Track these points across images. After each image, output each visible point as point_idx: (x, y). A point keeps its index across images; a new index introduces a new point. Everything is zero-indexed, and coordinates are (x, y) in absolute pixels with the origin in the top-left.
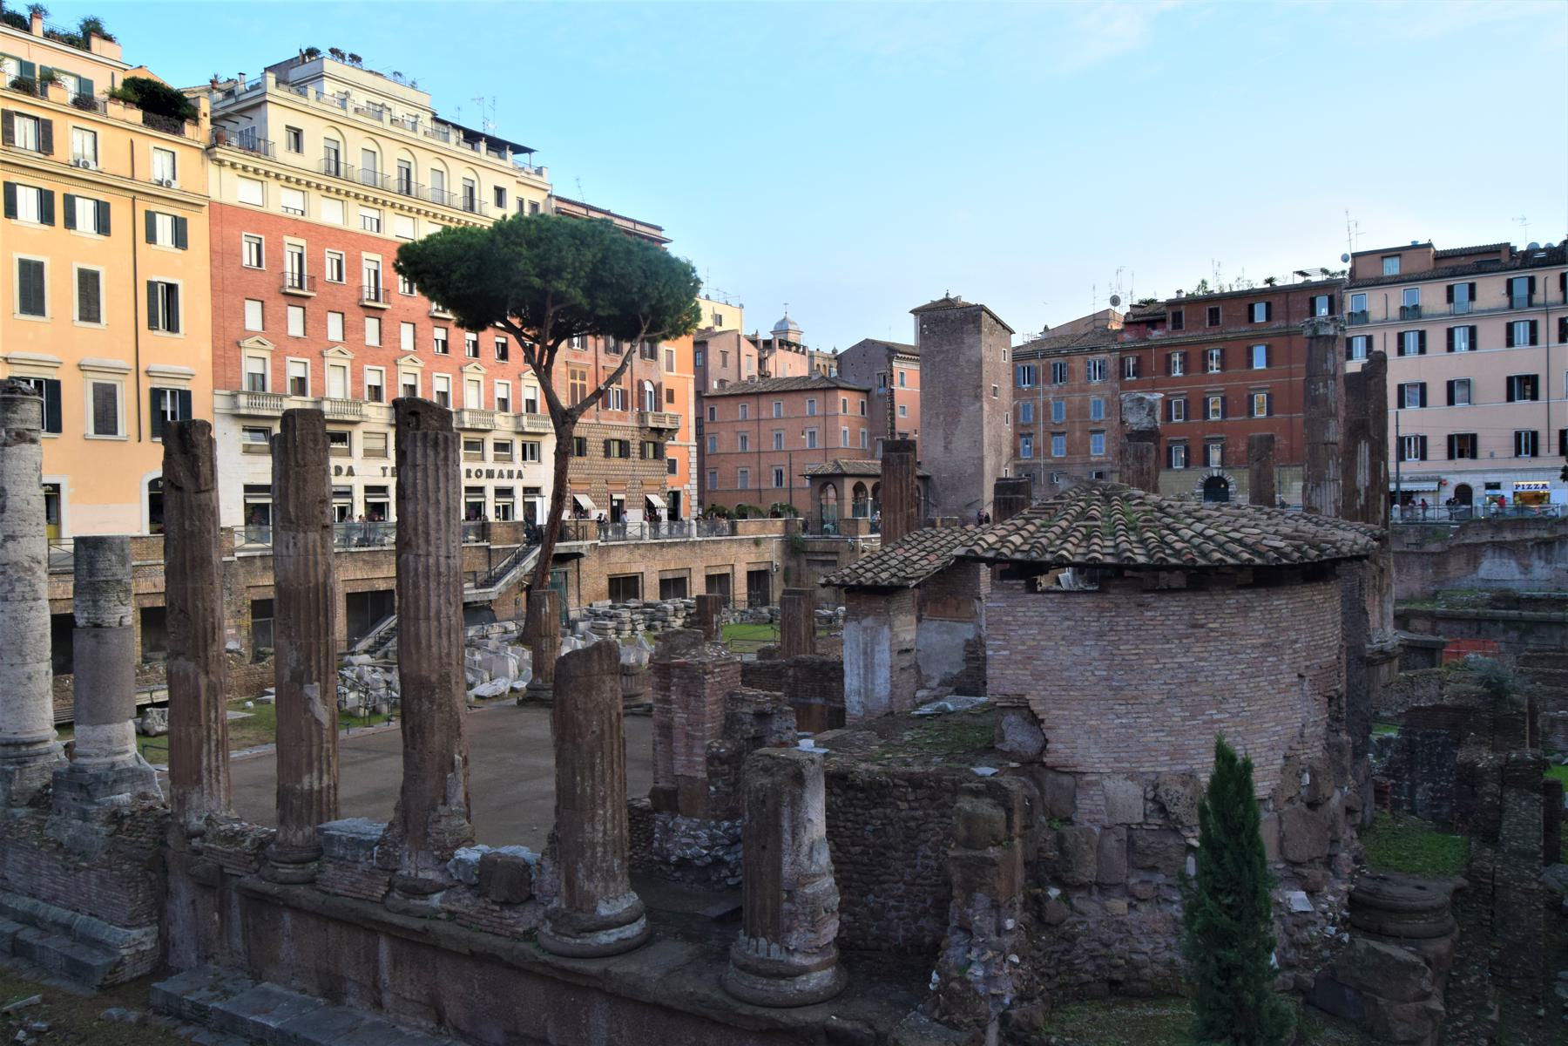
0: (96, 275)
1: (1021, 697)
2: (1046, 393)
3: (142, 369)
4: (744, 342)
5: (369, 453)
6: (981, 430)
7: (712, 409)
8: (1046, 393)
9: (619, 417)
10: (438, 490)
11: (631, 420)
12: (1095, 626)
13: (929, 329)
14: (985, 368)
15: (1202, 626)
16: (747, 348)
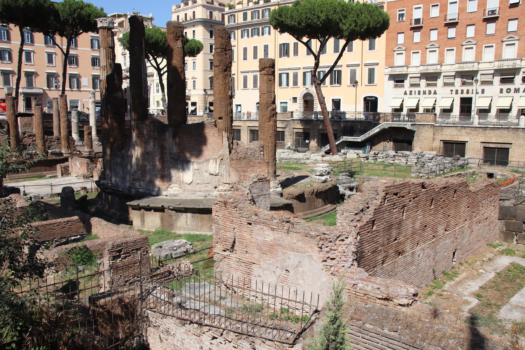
3: (363, 65)
5: (445, 84)
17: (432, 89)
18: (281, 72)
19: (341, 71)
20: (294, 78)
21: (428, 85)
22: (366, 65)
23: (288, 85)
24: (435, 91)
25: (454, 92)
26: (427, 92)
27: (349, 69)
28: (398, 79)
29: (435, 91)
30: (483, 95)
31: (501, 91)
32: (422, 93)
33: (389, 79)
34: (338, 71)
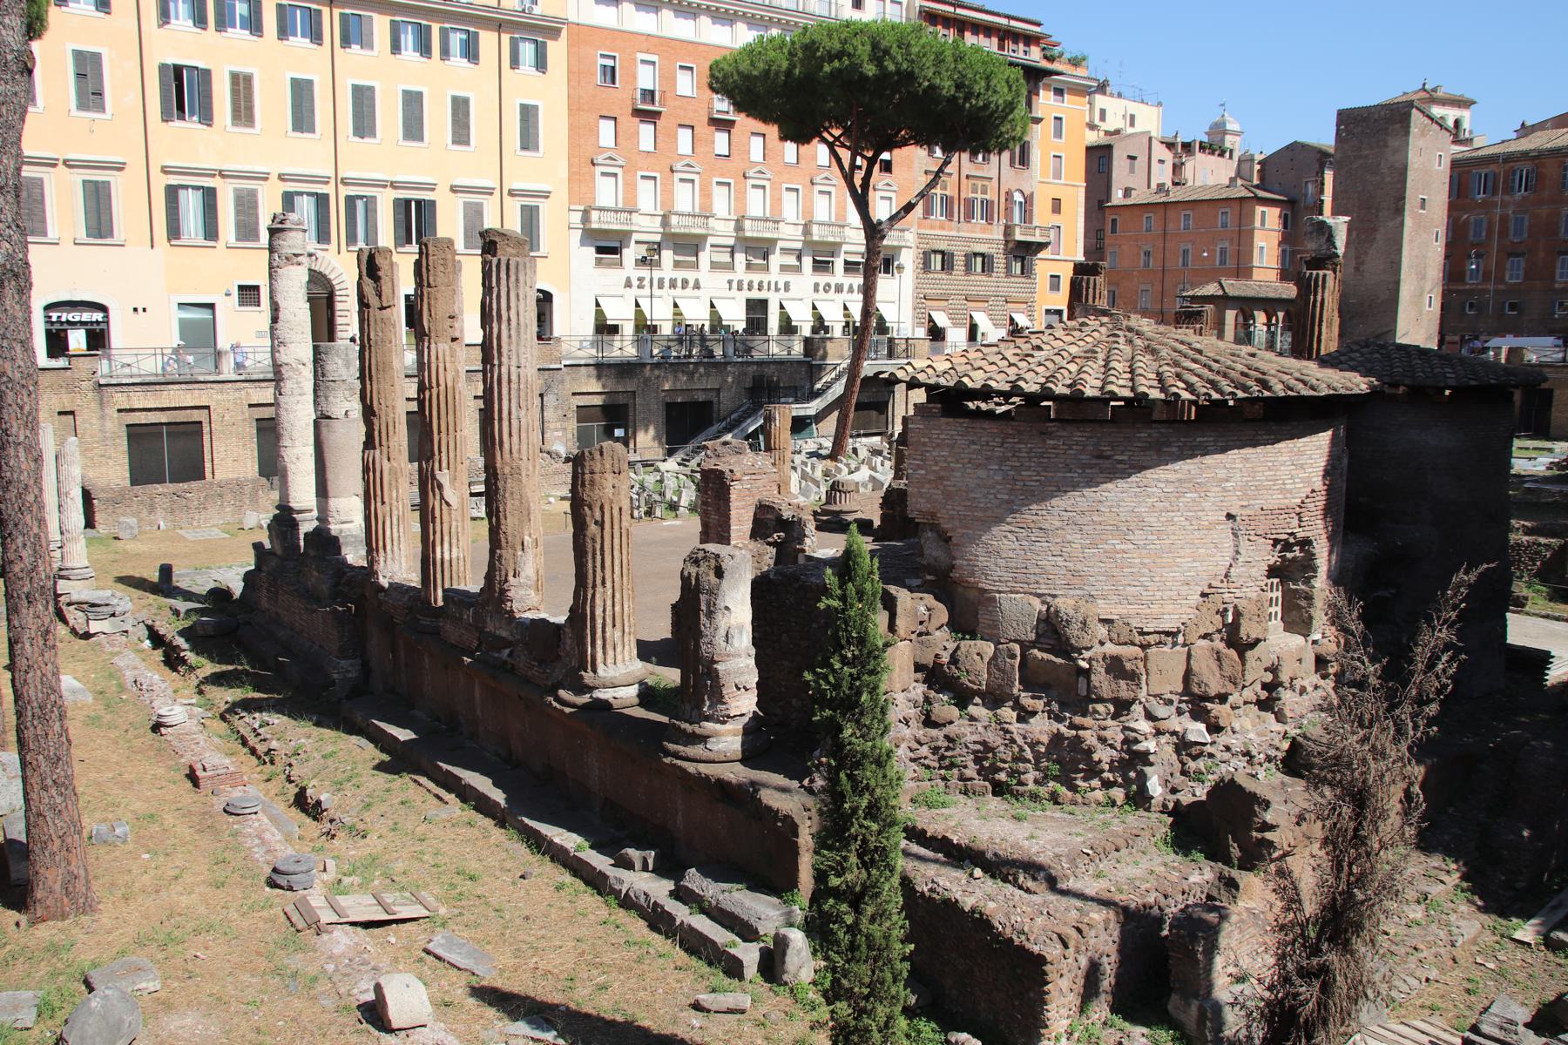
0: (466, 101)
1: (933, 515)
2: (1504, 205)
4: (1155, 143)
5: (715, 266)
6: (1400, 250)
7: (1114, 221)
8: (1504, 205)
9: (983, 231)
10: (509, 308)
11: (997, 233)
12: (998, 452)
13: (1346, 130)
14: (1411, 176)
15: (1108, 457)
16: (1159, 151)
17: (690, 275)
18: (174, 180)
19: (433, 203)
20: (238, 213)
21: (677, 264)
22: (511, 193)
23: (211, 232)
24: (697, 281)
25: (735, 285)
26: (679, 284)
27: (461, 199)
28: (608, 247)
29: (697, 281)
30: (787, 295)
31: (816, 287)
32: (667, 284)
33: (583, 243)
34: (418, 202)
